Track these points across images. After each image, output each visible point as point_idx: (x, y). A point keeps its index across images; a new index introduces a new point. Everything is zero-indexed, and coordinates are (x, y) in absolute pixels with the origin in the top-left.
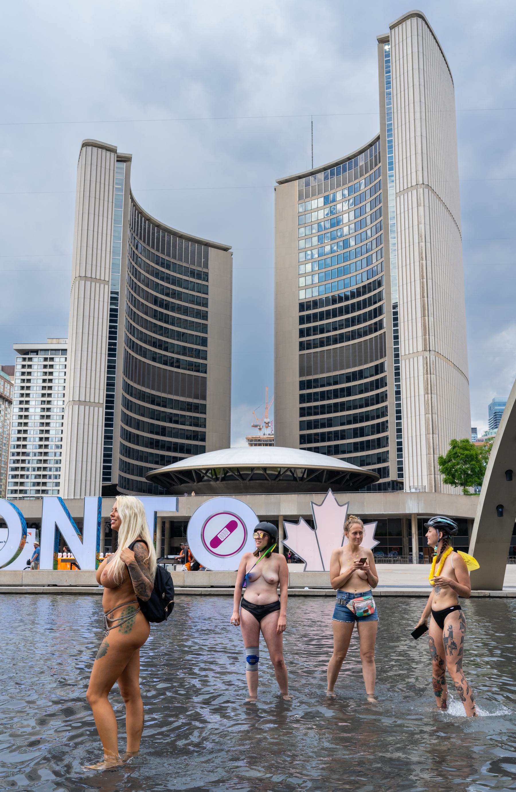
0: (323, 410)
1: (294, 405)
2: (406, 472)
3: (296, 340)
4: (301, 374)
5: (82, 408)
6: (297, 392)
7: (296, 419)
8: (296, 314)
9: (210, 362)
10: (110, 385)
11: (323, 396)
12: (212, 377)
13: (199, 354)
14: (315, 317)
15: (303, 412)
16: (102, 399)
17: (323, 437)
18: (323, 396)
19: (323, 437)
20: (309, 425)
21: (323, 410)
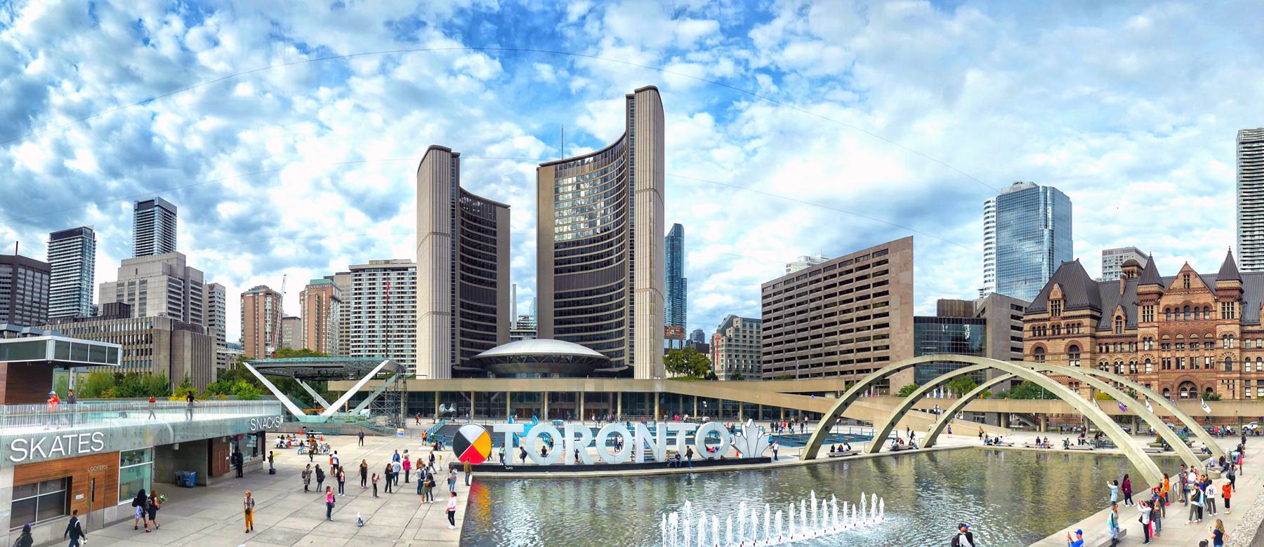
0: (569, 313)
1: (551, 309)
2: (636, 360)
3: (553, 267)
6: (553, 301)
7: (551, 318)
8: (553, 250)
9: (498, 281)
11: (569, 304)
12: (499, 290)
13: (491, 275)
14: (565, 254)
15: (556, 314)
17: (568, 330)
18: (569, 304)
19: (568, 330)
20: (561, 322)
21: (569, 313)
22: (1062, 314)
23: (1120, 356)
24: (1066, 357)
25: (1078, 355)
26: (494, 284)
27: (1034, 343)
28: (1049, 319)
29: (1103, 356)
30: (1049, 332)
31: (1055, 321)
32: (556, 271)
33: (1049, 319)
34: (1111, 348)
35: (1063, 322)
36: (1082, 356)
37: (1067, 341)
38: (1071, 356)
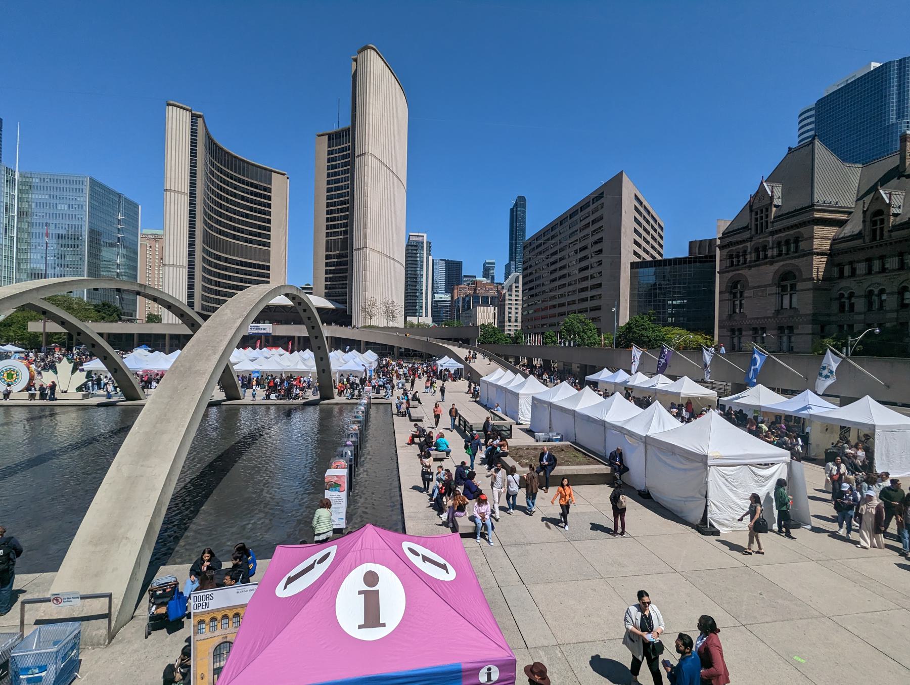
4: (327, 251)
5: (171, 268)
10: (191, 255)
16: (186, 263)
22: (770, 229)
23: (879, 279)
24: (774, 289)
25: (793, 287)
26: (268, 245)
27: (731, 274)
28: (750, 239)
29: (844, 283)
30: (750, 257)
31: (760, 240)
32: (328, 235)
33: (750, 239)
34: (861, 268)
35: (770, 239)
36: (800, 286)
37: (776, 266)
38: (784, 289)
